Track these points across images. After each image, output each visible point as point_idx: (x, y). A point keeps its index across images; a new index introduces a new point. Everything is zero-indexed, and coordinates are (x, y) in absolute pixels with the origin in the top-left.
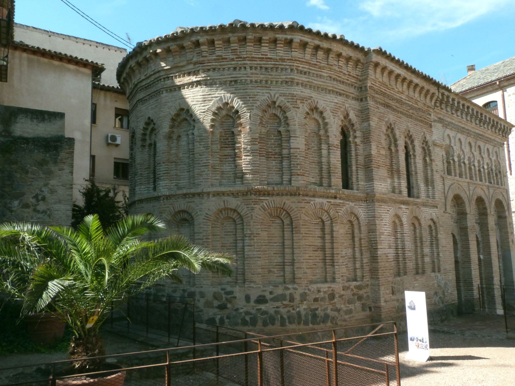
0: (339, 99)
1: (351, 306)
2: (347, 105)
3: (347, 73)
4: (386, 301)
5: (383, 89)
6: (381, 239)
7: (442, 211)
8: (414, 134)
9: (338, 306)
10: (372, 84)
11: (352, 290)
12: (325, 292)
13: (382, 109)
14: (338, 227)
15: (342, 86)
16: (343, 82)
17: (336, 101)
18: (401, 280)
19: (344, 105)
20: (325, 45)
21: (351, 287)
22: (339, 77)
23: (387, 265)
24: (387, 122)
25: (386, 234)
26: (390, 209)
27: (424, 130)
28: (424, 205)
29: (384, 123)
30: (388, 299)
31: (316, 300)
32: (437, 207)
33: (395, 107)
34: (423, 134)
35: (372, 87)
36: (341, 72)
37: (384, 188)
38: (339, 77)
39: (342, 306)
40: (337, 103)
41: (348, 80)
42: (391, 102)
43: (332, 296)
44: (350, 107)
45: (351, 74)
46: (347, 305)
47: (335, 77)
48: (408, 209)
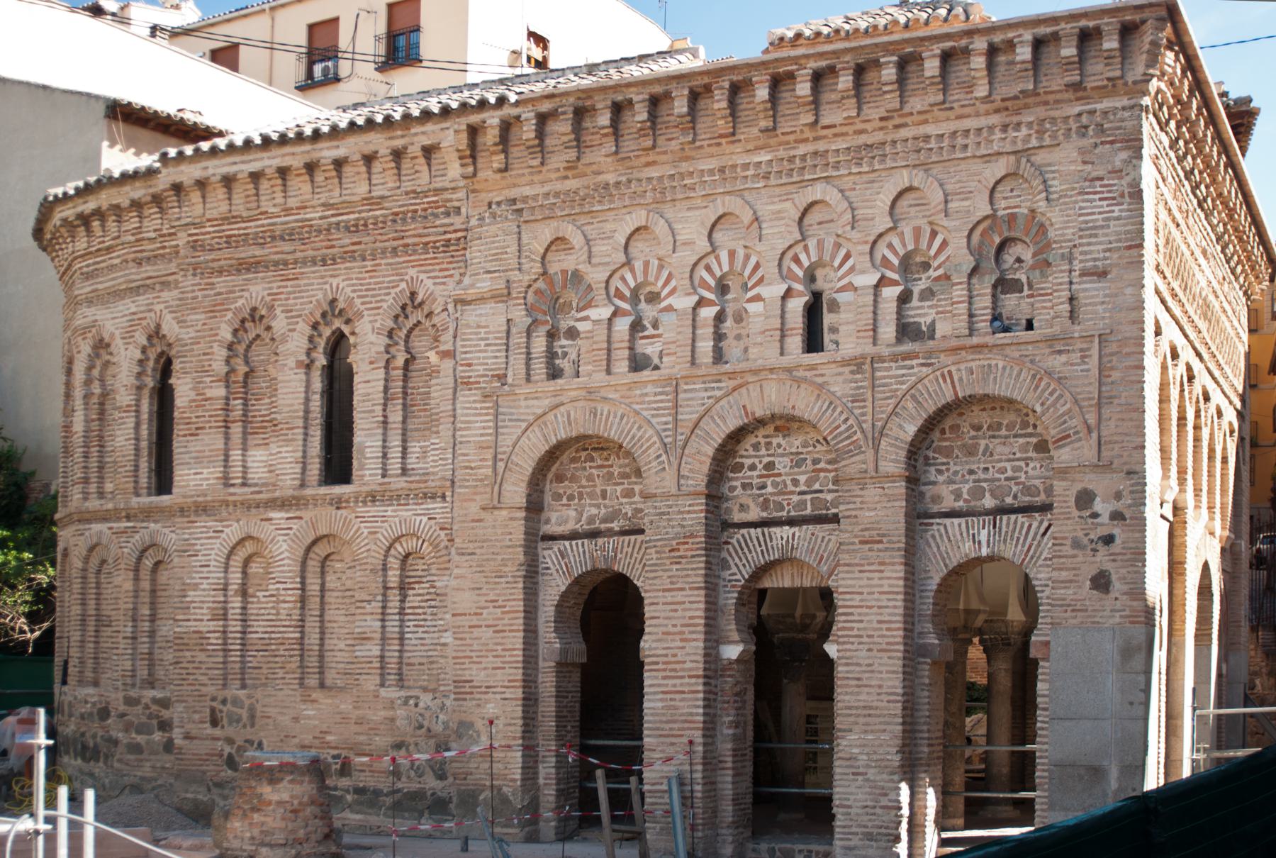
0: (129, 306)
1: (140, 739)
2: (158, 308)
3: (152, 235)
4: (187, 737)
5: (235, 229)
6: (188, 599)
7: (474, 508)
8: (358, 301)
9: (114, 734)
10: (190, 235)
11: (147, 707)
12: (94, 704)
13: (222, 283)
14: (120, 578)
15: (149, 268)
16: (155, 257)
17: (134, 309)
18: (250, 697)
19: (150, 311)
20: (89, 205)
21: (144, 701)
22: (141, 251)
23: (201, 656)
24: (239, 310)
25: (205, 586)
26: (228, 526)
27: (412, 272)
28: (373, 498)
29: (230, 315)
30: (194, 733)
31: (82, 717)
32: (444, 497)
33: (276, 257)
34: (403, 285)
35: (196, 241)
36: (143, 239)
37: (207, 479)
38: (141, 251)
39: (120, 735)
40: (134, 313)
41: (164, 247)
42: (258, 252)
43: (104, 713)
44: (166, 308)
45: (165, 232)
46: (134, 735)
47: (133, 256)
48: (301, 518)
